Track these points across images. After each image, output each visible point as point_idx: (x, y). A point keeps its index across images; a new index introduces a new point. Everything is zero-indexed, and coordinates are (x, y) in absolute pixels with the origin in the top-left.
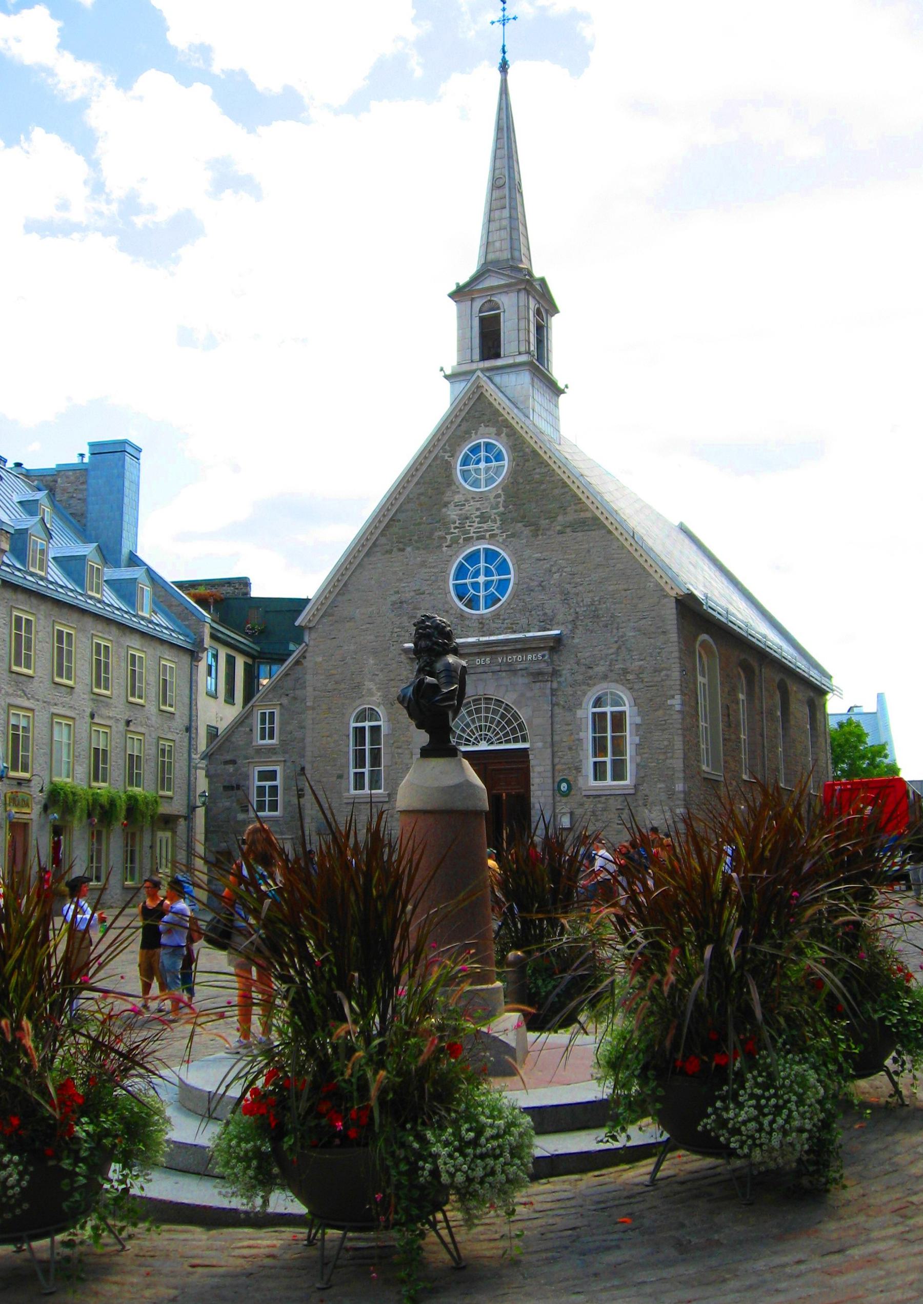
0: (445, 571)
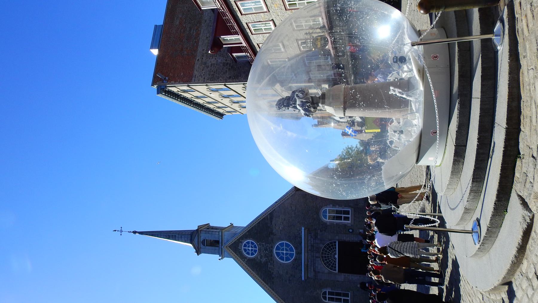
0: (281, 264)
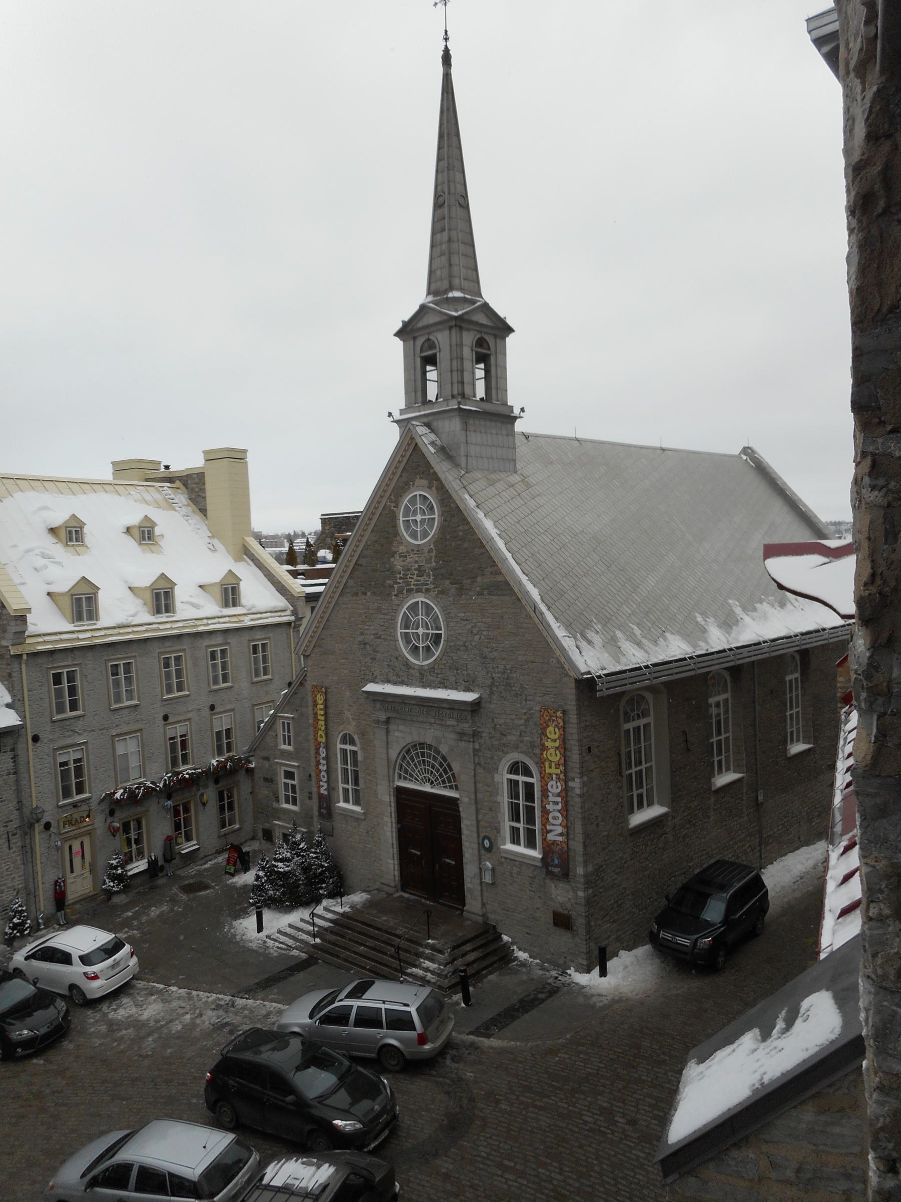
0: (394, 619)
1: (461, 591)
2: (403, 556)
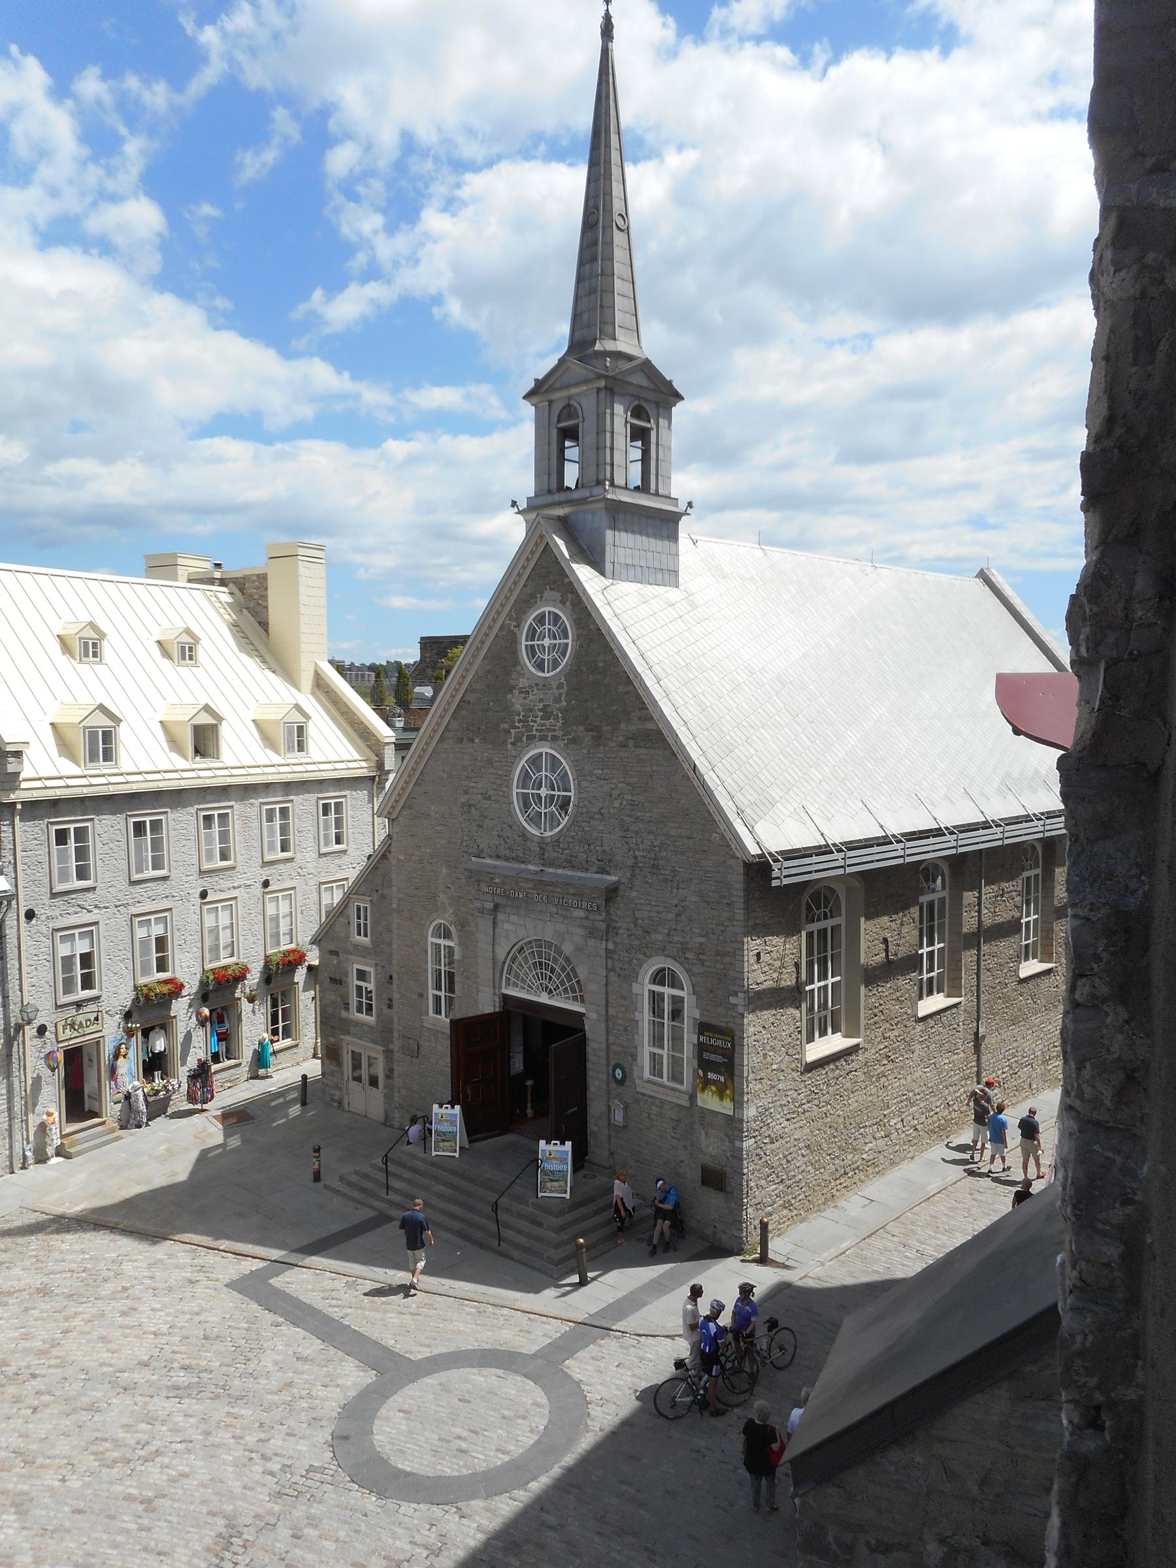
0: (509, 774)
1: (598, 740)
2: (525, 692)
